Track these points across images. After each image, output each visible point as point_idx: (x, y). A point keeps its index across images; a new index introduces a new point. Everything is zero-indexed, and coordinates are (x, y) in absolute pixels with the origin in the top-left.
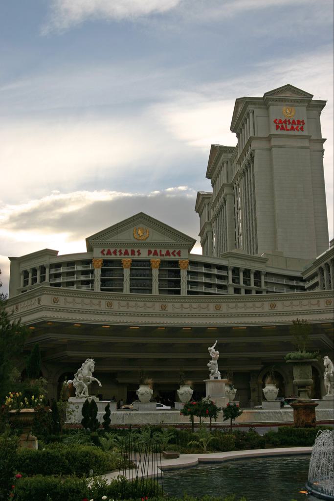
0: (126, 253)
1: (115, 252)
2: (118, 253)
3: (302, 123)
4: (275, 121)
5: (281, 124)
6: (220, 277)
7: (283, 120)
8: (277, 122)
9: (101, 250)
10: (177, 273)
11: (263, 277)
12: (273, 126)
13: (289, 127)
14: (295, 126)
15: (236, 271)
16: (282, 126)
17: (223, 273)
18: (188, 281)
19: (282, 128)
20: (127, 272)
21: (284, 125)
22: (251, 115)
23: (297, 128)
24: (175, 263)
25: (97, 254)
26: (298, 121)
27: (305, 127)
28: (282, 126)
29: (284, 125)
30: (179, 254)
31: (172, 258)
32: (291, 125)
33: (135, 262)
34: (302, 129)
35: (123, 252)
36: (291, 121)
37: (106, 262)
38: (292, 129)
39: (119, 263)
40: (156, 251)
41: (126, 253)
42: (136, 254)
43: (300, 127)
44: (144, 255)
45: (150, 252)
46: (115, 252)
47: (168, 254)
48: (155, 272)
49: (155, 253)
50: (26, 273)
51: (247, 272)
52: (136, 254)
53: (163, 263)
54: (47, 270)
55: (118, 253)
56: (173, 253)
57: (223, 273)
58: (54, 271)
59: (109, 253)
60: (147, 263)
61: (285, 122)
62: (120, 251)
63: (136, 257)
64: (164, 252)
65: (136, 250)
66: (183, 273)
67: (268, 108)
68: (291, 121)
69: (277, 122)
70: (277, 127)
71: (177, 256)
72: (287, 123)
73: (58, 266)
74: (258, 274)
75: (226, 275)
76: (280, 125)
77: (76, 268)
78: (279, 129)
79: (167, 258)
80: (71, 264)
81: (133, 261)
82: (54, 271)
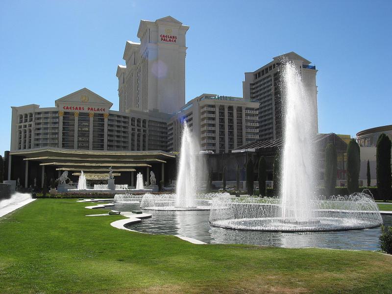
0: (77, 109)
1: (70, 108)
2: (72, 109)
5: (164, 38)
6: (125, 122)
9: (63, 106)
10: (103, 120)
11: (147, 123)
13: (168, 39)
14: (171, 39)
15: (133, 120)
17: (126, 120)
18: (108, 124)
19: (165, 40)
20: (76, 118)
21: (166, 38)
22: (148, 31)
24: (102, 115)
25: (62, 110)
29: (166, 38)
30: (104, 110)
31: (100, 112)
33: (81, 114)
34: (175, 41)
35: (75, 108)
37: (65, 113)
38: (170, 40)
39: (73, 114)
40: (92, 108)
41: (77, 109)
42: (82, 109)
44: (86, 111)
45: (89, 109)
46: (70, 108)
47: (98, 110)
48: (91, 119)
49: (92, 109)
50: (21, 117)
51: (139, 121)
52: (82, 109)
53: (95, 115)
54: (33, 116)
55: (72, 109)
56: (101, 110)
57: (126, 120)
58: (37, 116)
59: (67, 108)
60: (88, 115)
62: (73, 107)
63: (82, 111)
64: (96, 109)
65: (82, 107)
66: (106, 120)
70: (162, 39)
71: (103, 111)
73: (39, 113)
74: (144, 121)
75: (128, 121)
76: (164, 38)
77: (49, 115)
79: (98, 112)
80: (47, 113)
81: (80, 113)
82: (37, 116)
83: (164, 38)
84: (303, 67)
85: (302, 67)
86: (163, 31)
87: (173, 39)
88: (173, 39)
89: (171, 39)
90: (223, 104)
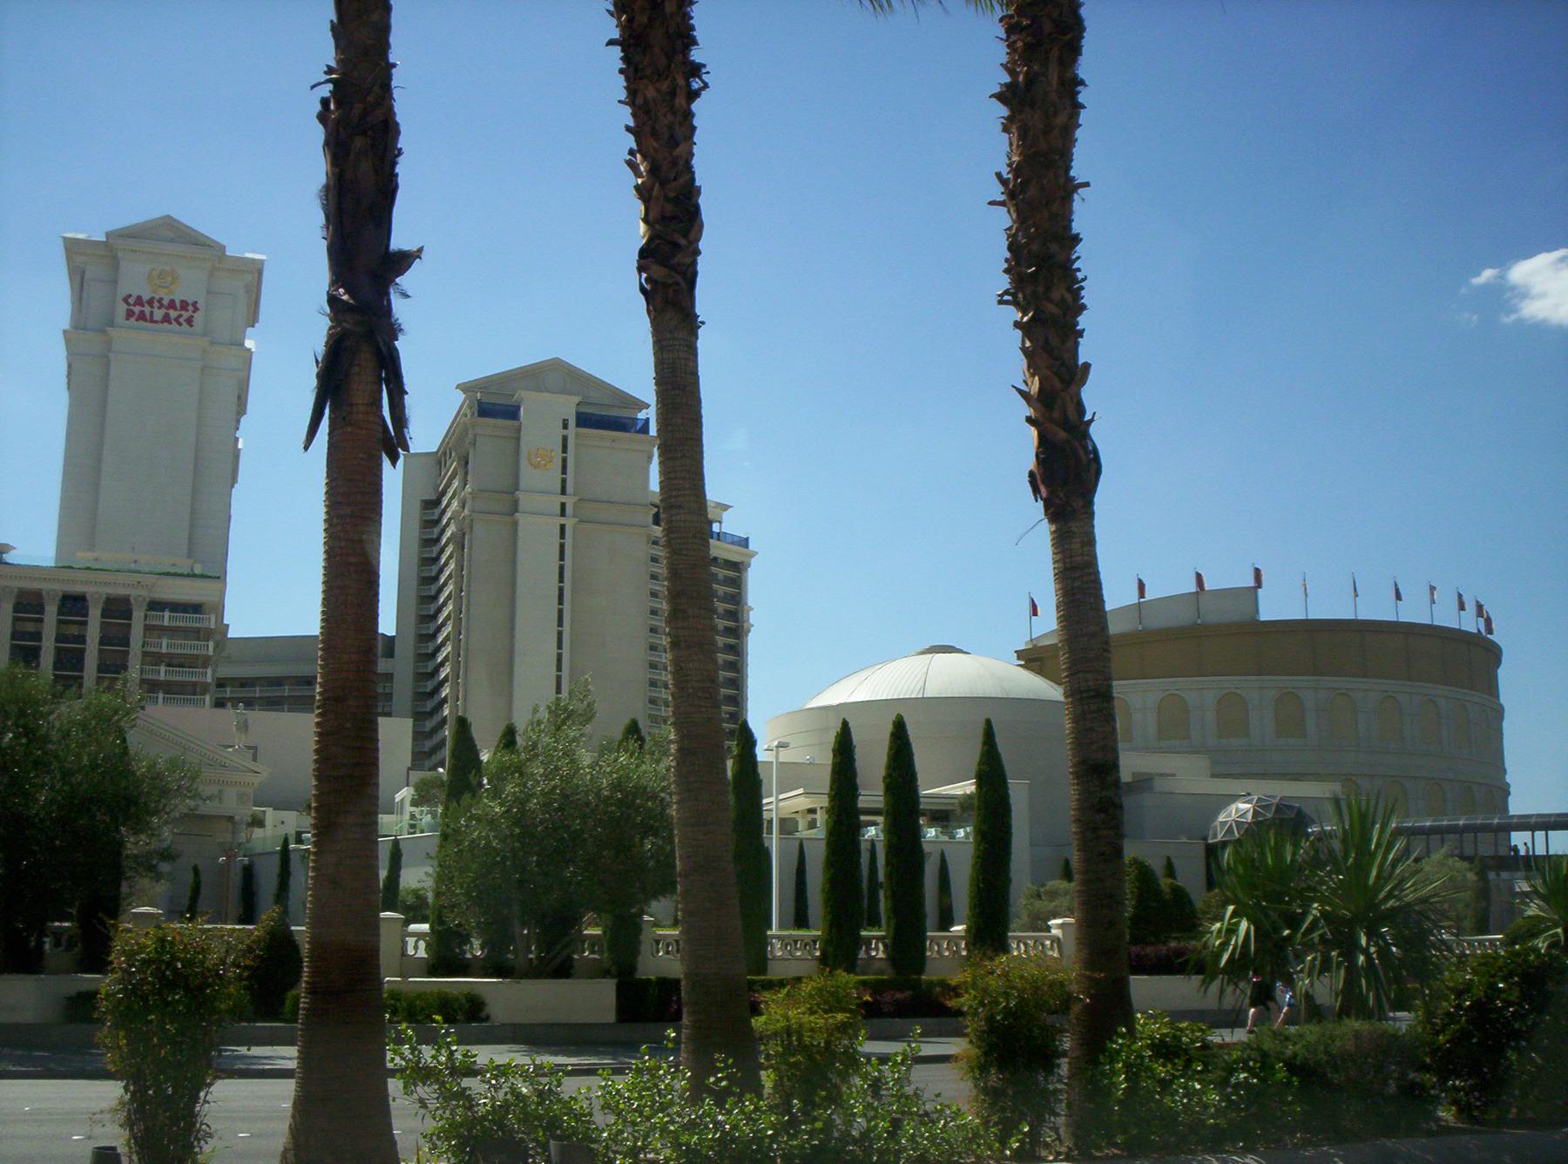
3: (190, 308)
4: (126, 300)
5: (139, 310)
7: (146, 298)
8: (131, 301)
12: (122, 309)
13: (159, 314)
14: (173, 314)
16: (142, 313)
19: (142, 317)
21: (147, 309)
23: (177, 320)
26: (184, 305)
27: (199, 318)
28: (142, 313)
29: (147, 309)
32: (163, 311)
34: (189, 321)
36: (166, 302)
38: (166, 319)
43: (186, 315)
61: (150, 302)
67: (116, 267)
68: (166, 302)
69: (131, 301)
70: (130, 314)
72: (156, 304)
78: (133, 320)
83: (137, 309)
84: (578, 425)
85: (572, 423)
86: (136, 279)
87: (180, 312)
88: (180, 312)
89: (173, 314)
90: (36, 586)
